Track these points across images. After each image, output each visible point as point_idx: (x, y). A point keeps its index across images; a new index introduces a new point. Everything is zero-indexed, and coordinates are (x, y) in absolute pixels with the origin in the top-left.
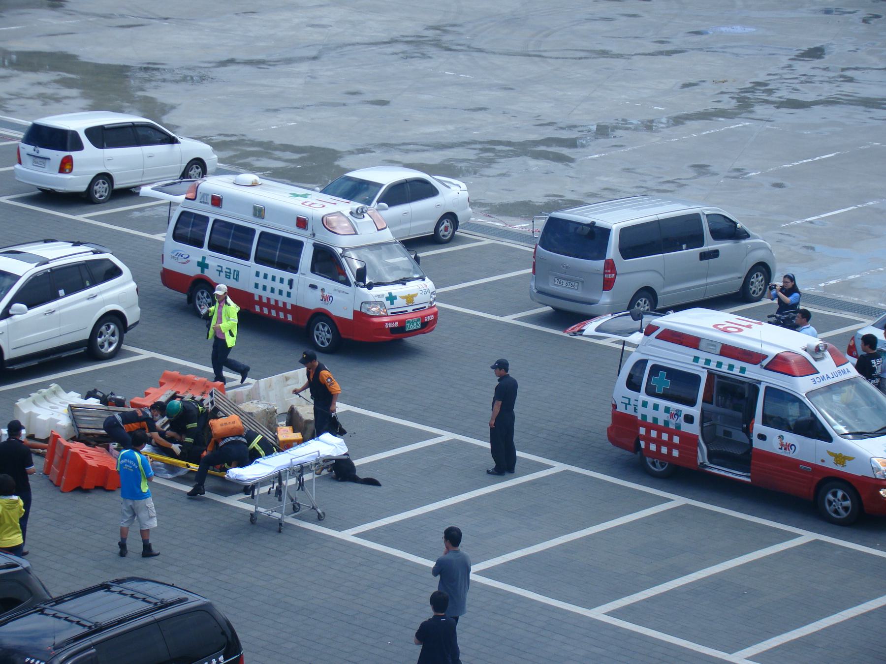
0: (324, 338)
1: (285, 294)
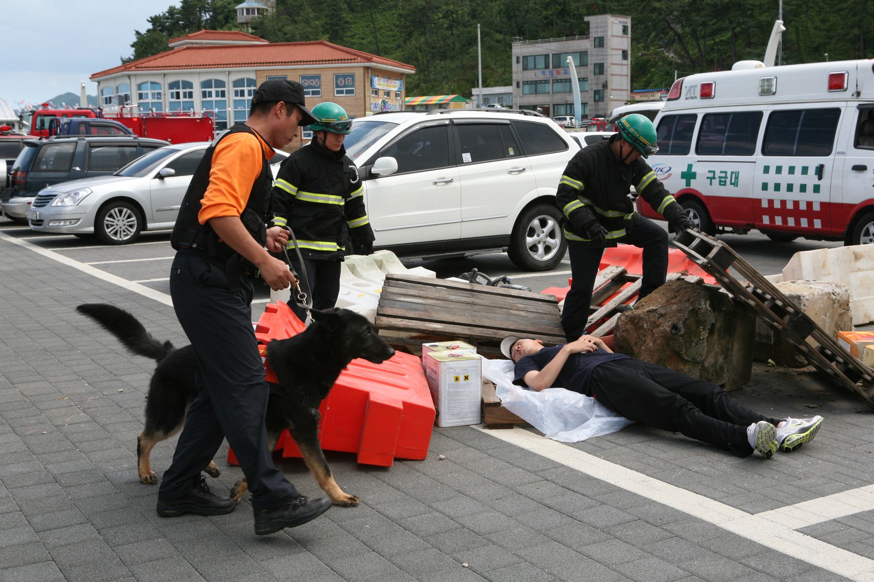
1: (810, 189)
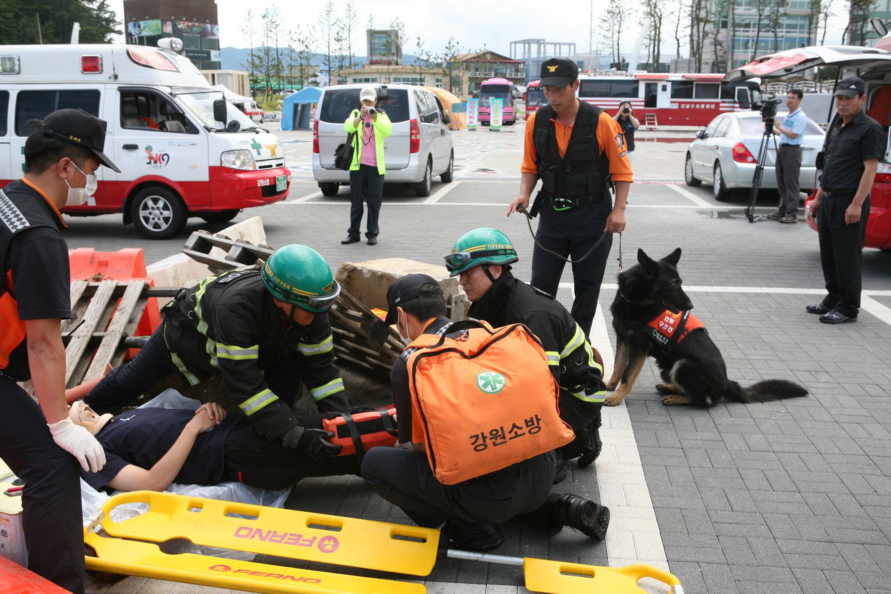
0: (159, 219)
